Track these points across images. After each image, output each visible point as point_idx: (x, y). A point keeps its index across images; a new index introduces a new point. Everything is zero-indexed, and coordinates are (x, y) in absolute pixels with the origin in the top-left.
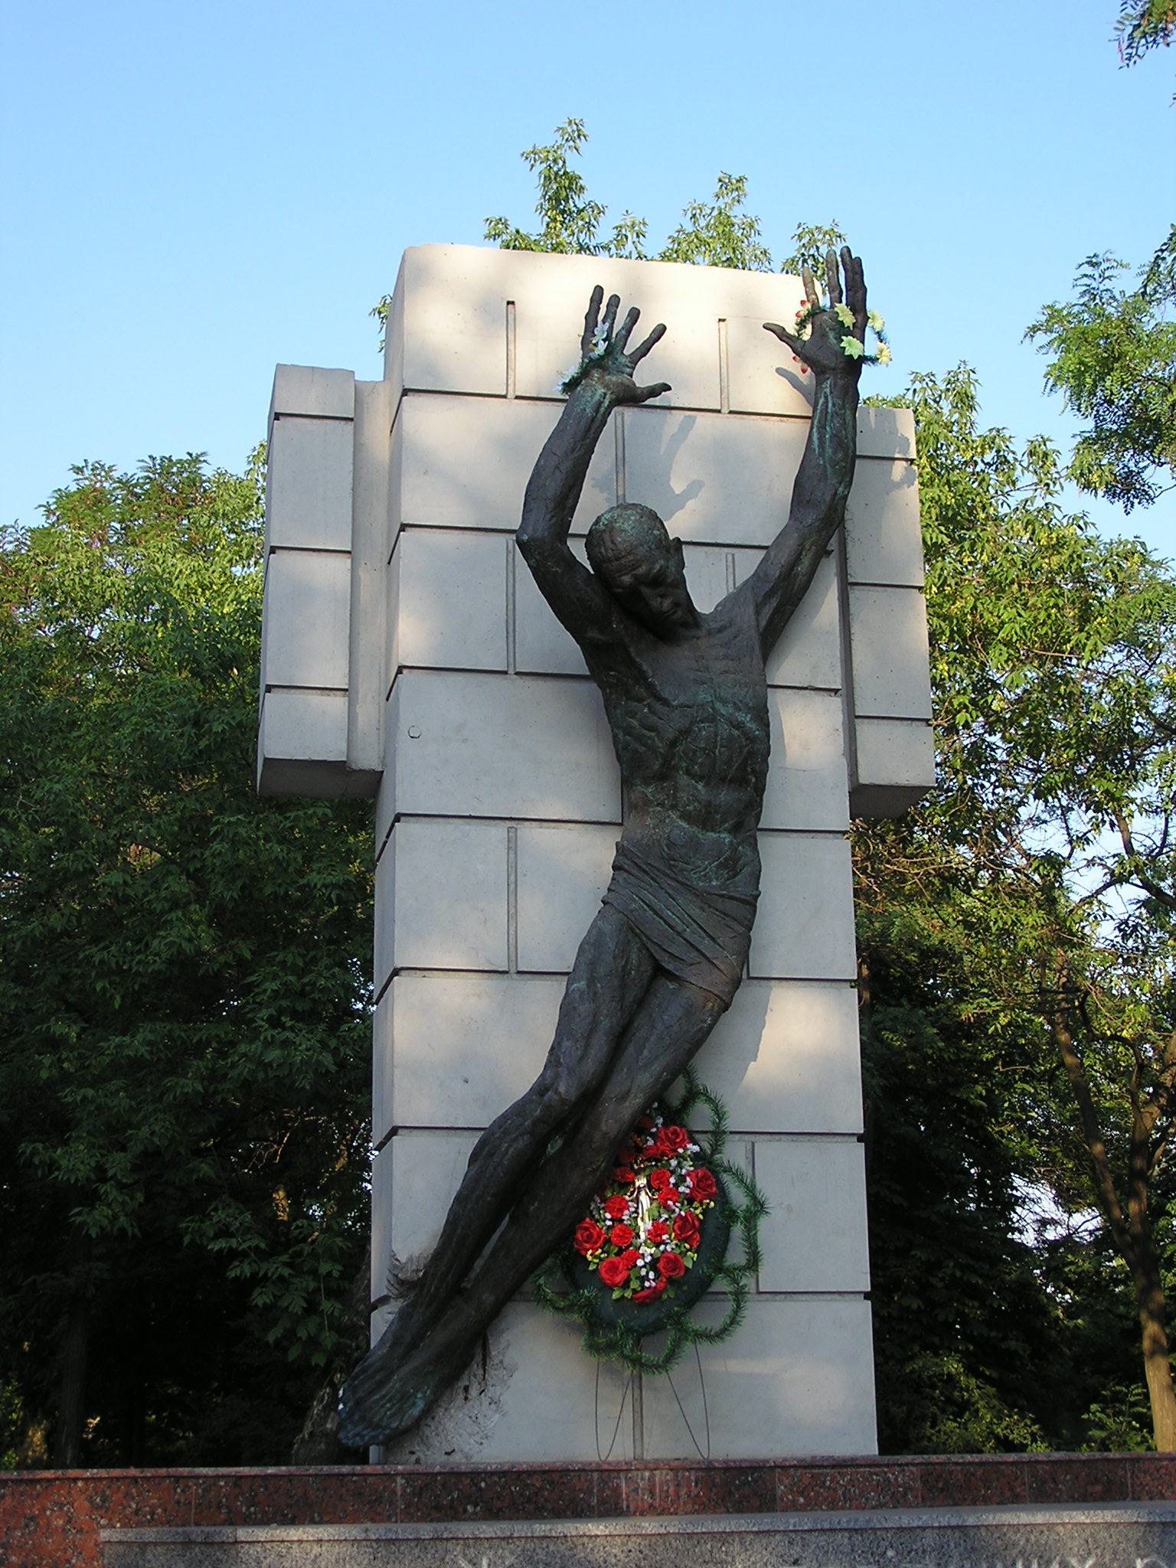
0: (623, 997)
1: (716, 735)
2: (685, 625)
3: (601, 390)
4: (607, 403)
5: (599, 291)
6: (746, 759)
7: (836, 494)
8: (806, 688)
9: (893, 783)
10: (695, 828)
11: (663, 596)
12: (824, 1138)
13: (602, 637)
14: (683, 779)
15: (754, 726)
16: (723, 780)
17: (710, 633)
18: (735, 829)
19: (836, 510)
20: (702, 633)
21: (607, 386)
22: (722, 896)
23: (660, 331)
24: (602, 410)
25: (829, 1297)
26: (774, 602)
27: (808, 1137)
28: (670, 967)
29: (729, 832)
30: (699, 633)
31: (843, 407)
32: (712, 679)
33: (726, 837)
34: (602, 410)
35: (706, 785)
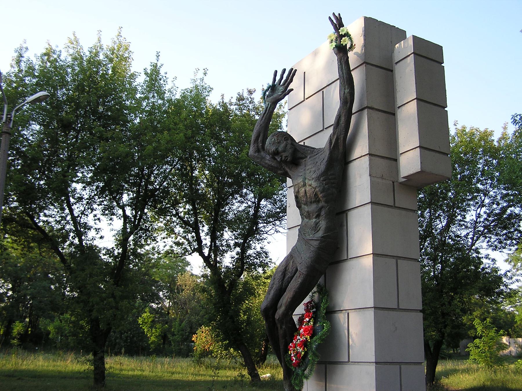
0: (284, 277)
1: (305, 191)
2: (302, 158)
3: (268, 103)
4: (269, 106)
5: (276, 72)
6: (316, 195)
7: (344, 93)
8: (361, 157)
9: (409, 174)
10: (308, 220)
11: (281, 156)
12: (367, 310)
13: (282, 172)
14: (303, 206)
15: (315, 183)
16: (311, 202)
17: (310, 158)
18: (318, 216)
19: (346, 98)
20: (308, 157)
21: (268, 101)
22: (310, 240)
23: (296, 70)
24: (268, 109)
25: (367, 364)
26: (335, 136)
27: (363, 309)
28: (297, 265)
29: (316, 217)
30: (306, 159)
31: (341, 64)
32: (305, 174)
33: (314, 220)
34: (268, 109)
35: (307, 206)
